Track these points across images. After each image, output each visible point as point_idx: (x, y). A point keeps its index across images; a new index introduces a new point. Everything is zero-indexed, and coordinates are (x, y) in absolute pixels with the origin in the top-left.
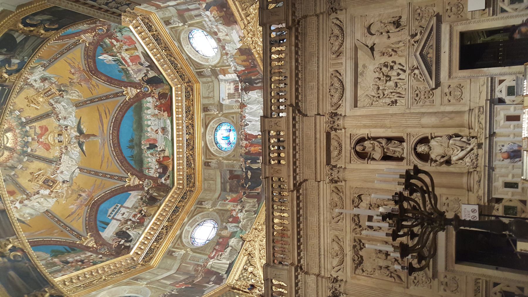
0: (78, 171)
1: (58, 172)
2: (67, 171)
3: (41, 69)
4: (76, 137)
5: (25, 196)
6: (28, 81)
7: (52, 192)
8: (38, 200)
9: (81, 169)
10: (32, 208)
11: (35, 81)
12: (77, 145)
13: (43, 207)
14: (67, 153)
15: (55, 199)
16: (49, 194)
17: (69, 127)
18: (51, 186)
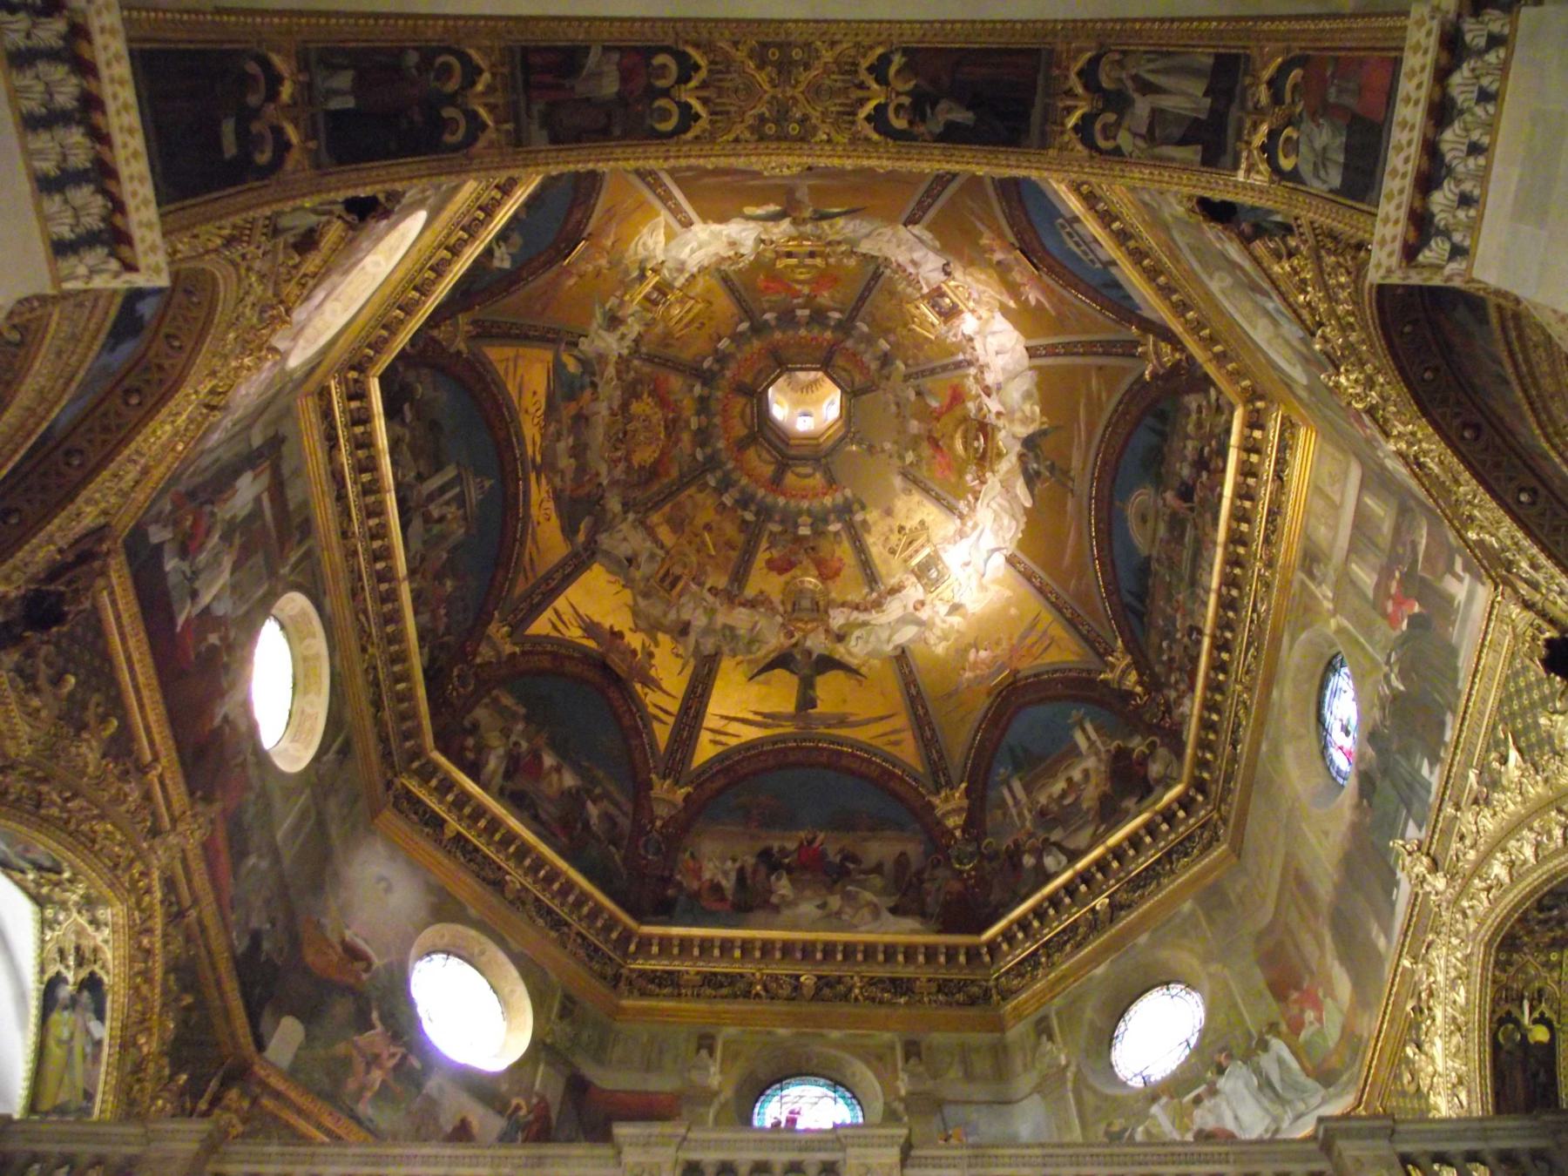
0: (916, 229)
1: (911, 269)
2: (911, 250)
3: (584, 344)
4: (795, 222)
5: (972, 371)
6: (625, 352)
7: (973, 311)
8: (992, 348)
9: (911, 221)
10: (1013, 376)
11: (623, 337)
12: (825, 225)
13: (1013, 349)
14: (853, 243)
15: (998, 316)
16: (980, 318)
17: (763, 237)
18: (955, 306)
